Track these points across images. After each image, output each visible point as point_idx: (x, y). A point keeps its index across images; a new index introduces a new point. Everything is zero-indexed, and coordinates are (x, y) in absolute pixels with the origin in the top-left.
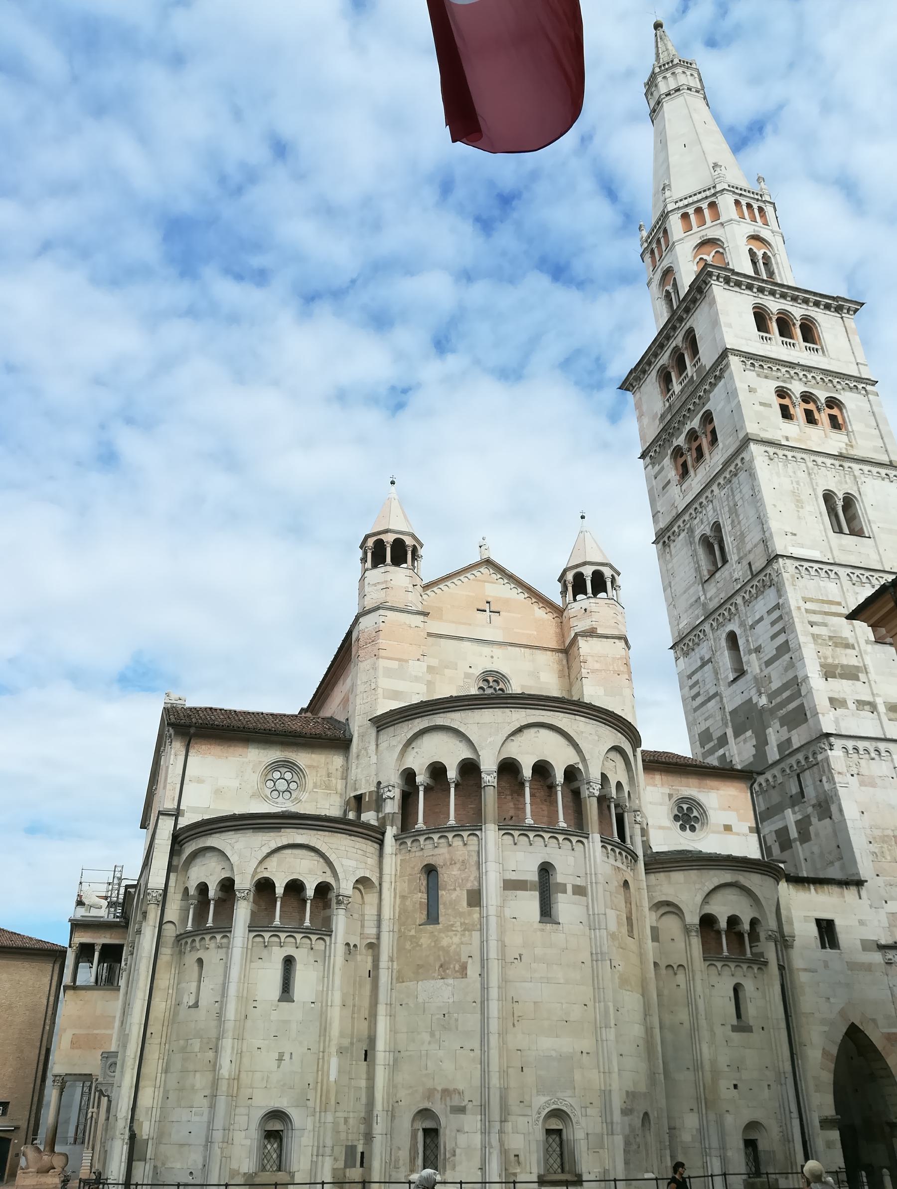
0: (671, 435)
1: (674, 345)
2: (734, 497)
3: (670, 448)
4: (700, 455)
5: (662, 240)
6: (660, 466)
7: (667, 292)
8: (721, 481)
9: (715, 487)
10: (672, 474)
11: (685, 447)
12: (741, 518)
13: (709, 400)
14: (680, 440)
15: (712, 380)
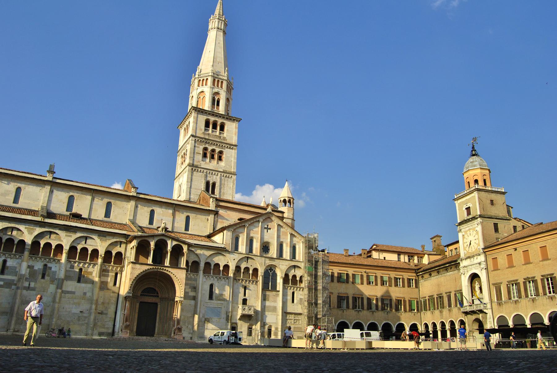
0: (206, 142)
1: (217, 119)
2: (224, 182)
3: (204, 145)
4: (212, 157)
5: (220, 83)
6: (198, 146)
7: (214, 97)
8: (222, 174)
9: (219, 174)
10: (201, 152)
11: (209, 150)
12: (225, 189)
13: (225, 149)
14: (210, 148)
15: (229, 147)
